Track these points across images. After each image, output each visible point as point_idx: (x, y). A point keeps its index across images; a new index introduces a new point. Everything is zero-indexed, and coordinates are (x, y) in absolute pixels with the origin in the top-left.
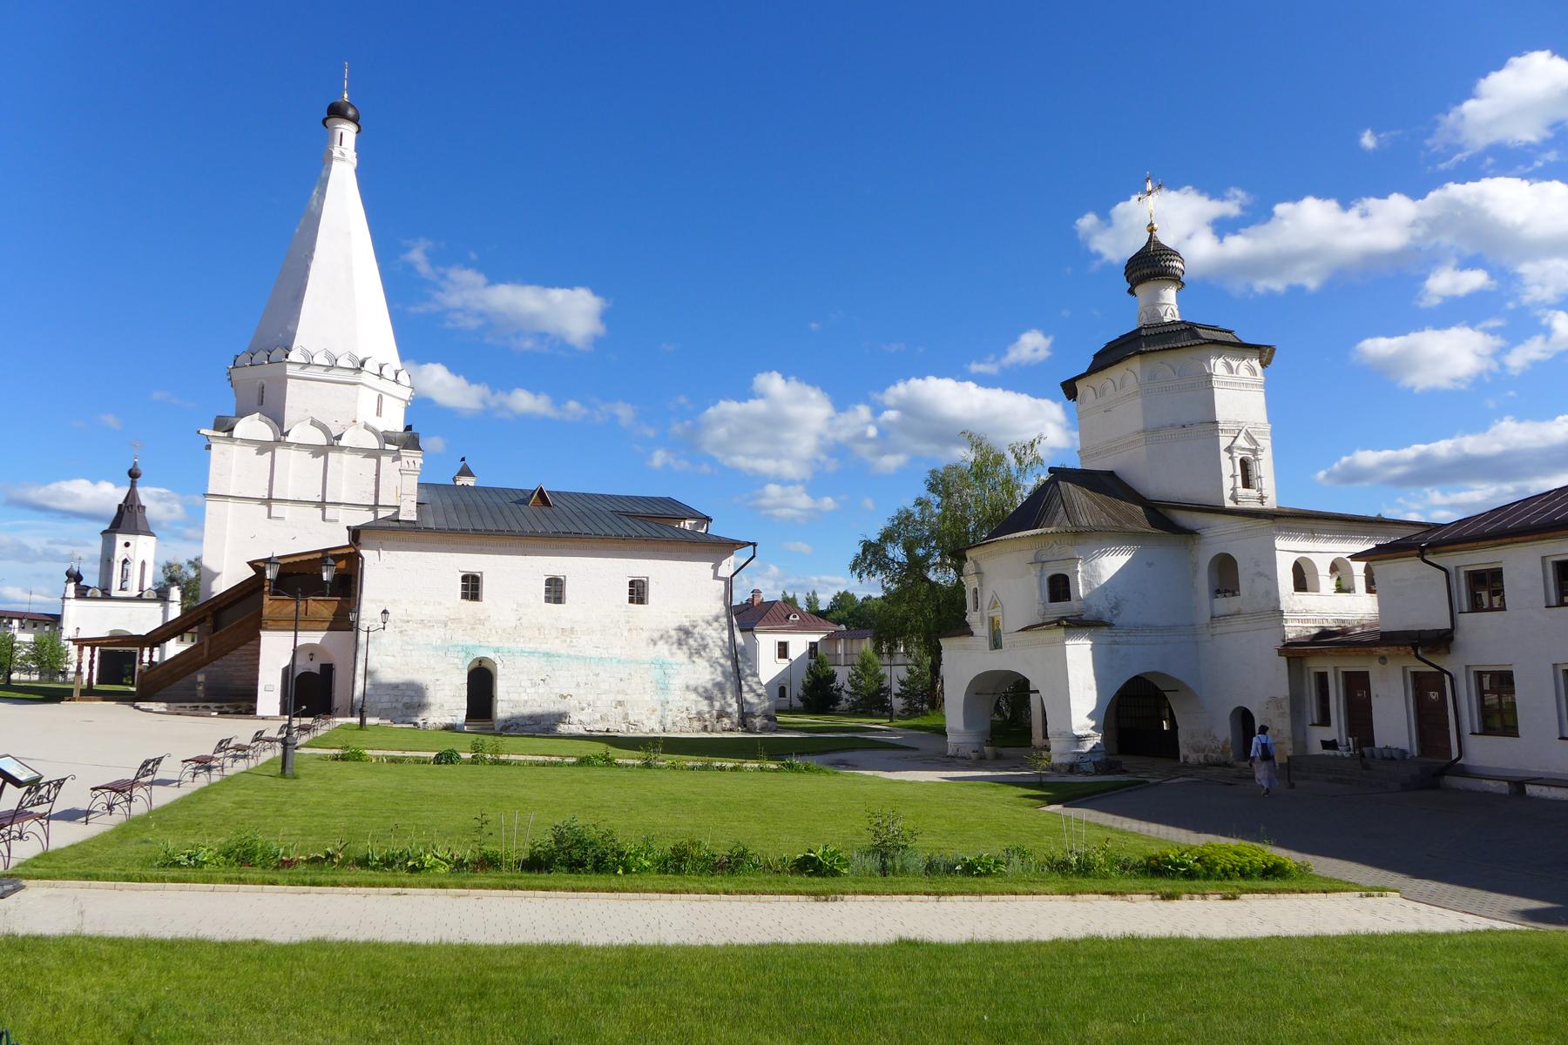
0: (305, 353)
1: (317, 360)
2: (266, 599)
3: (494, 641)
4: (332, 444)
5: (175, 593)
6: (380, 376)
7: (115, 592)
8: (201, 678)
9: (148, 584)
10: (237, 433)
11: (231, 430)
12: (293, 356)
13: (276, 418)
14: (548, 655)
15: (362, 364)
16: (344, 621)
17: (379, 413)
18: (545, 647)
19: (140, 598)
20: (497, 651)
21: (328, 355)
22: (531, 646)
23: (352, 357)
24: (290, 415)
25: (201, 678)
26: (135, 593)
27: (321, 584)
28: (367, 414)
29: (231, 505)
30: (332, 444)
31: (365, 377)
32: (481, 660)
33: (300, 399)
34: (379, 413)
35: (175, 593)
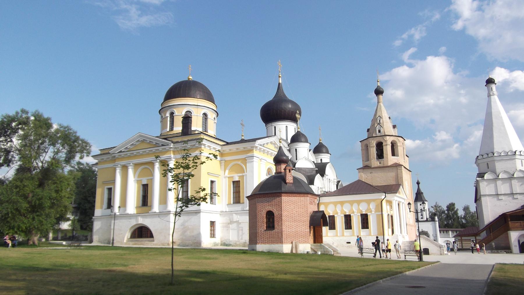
0: (498, 153)
1: (502, 154)
2: (510, 222)
4: (511, 177)
5: (436, 218)
6: (521, 155)
7: (420, 219)
8: (493, 244)
10: (485, 178)
11: (483, 177)
12: (495, 155)
13: (494, 172)
15: (515, 152)
17: (522, 166)
19: (427, 221)
21: (505, 152)
24: (498, 171)
25: (493, 244)
26: (425, 219)
30: (511, 177)
31: (517, 157)
33: (500, 166)
34: (522, 166)
35: (436, 218)
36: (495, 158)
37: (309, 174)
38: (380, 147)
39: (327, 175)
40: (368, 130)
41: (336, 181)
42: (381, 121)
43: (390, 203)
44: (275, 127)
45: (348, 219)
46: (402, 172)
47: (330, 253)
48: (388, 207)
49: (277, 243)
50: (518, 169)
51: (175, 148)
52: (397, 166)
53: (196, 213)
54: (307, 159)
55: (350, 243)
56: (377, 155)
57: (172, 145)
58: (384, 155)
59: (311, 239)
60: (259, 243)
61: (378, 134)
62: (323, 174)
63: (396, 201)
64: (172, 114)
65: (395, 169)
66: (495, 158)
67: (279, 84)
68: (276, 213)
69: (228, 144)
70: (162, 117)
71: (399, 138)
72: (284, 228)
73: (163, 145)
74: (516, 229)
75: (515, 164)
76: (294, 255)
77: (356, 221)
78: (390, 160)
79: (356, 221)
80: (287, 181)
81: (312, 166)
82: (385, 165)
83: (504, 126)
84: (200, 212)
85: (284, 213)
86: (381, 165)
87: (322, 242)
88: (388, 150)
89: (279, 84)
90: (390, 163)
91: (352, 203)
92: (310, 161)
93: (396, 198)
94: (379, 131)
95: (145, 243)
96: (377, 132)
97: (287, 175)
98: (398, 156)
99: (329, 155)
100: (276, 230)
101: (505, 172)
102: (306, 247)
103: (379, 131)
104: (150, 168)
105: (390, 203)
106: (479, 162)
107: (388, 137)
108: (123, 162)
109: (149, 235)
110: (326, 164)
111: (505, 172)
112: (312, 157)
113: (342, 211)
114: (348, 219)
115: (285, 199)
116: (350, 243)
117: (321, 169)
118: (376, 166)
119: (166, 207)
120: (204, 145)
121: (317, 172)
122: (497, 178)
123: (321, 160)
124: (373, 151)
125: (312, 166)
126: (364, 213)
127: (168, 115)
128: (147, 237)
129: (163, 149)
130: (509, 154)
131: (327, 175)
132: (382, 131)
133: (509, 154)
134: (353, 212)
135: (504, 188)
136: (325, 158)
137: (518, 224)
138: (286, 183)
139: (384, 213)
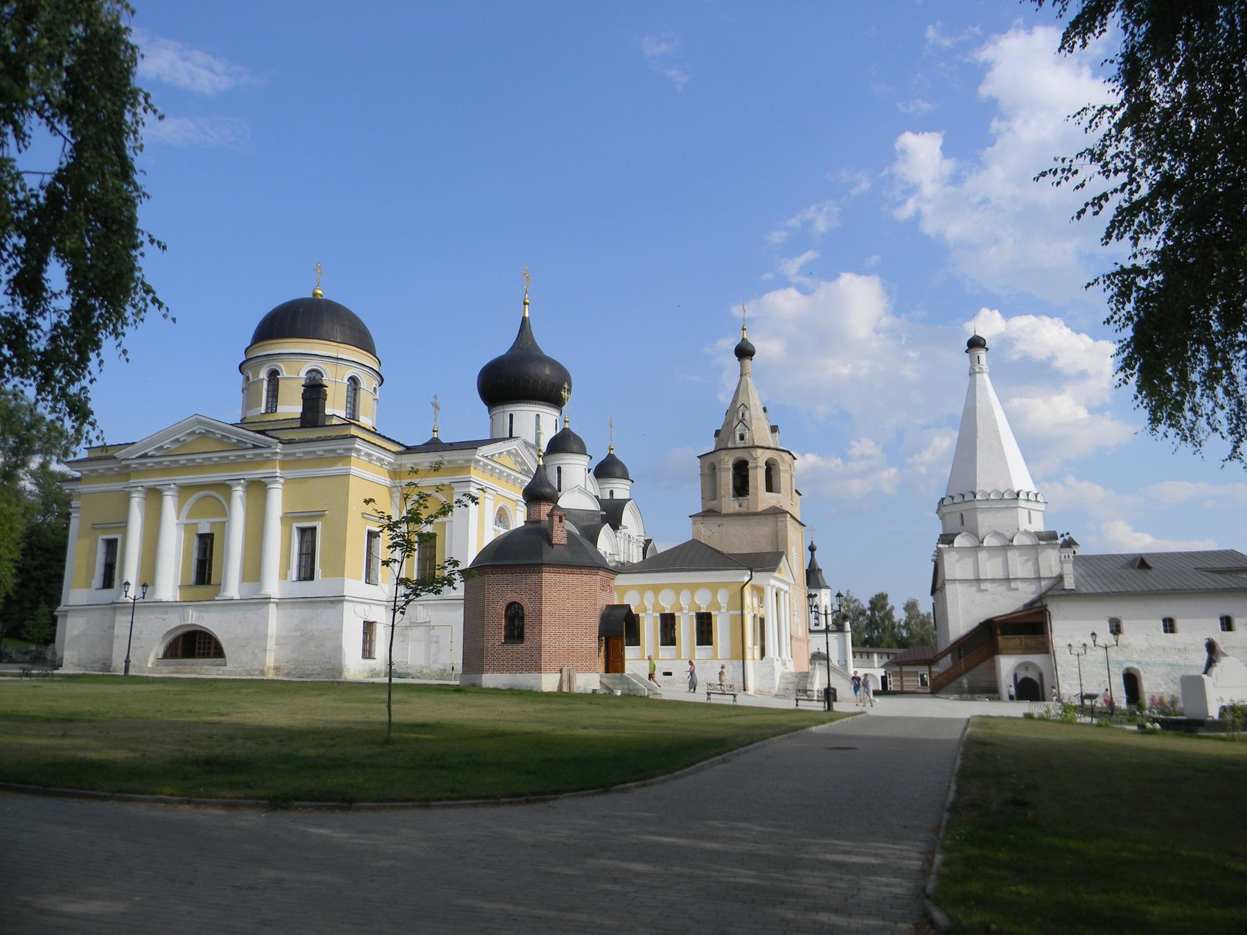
0: (984, 493)
1: (992, 497)
2: (1000, 638)
3: (1136, 657)
6: (1028, 500)
8: (965, 681)
9: (830, 622)
10: (956, 544)
12: (978, 497)
13: (974, 533)
14: (1171, 665)
16: (1044, 648)
18: (1169, 660)
20: (1139, 663)
21: (997, 492)
22: (1160, 660)
23: (1011, 492)
24: (982, 531)
25: (965, 681)
27: (1029, 627)
28: (1024, 525)
29: (958, 586)
30: (1008, 546)
31: (1022, 503)
32: (1128, 669)
33: (986, 522)
36: (978, 505)
37: (586, 523)
38: (741, 470)
39: (626, 528)
40: (717, 433)
41: (642, 539)
42: (747, 416)
43: (759, 591)
44: (511, 416)
45: (668, 623)
46: (786, 527)
47: (641, 693)
48: (755, 601)
49: (529, 671)
50: (1022, 529)
51: (285, 455)
52: (776, 513)
53: (332, 602)
54: (583, 491)
55: (670, 674)
56: (735, 488)
57: (279, 448)
58: (750, 489)
59: (600, 663)
60: (487, 672)
61: (739, 443)
62: (616, 524)
63: (773, 586)
64: (274, 374)
65: (770, 521)
66: (978, 505)
67: (524, 319)
68: (528, 607)
69: (409, 450)
70: (248, 378)
71: (783, 454)
72: (545, 640)
73: (255, 447)
74: (1011, 651)
75: (1017, 518)
76: (563, 697)
77: (686, 629)
78: (762, 499)
79: (686, 629)
80: (555, 541)
81: (593, 506)
82: (752, 510)
83: (999, 438)
84: (342, 601)
85: (546, 609)
86: (743, 510)
87: (622, 671)
88: (758, 477)
89: (524, 319)
90: (762, 507)
91: (677, 589)
92: (588, 494)
93: (773, 582)
94: (742, 438)
95: (203, 669)
96: (738, 437)
97: (555, 528)
98: (779, 492)
99: (629, 483)
100: (527, 643)
101: (996, 534)
102: (589, 680)
103: (742, 438)
104: (221, 498)
105: (759, 591)
106: (944, 510)
107: (760, 451)
108: (151, 481)
109: (212, 651)
110: (623, 502)
111: (996, 534)
112: (592, 486)
113: (656, 605)
114: (668, 623)
115: (549, 578)
116: (670, 674)
117: (612, 513)
118: (731, 511)
119: (260, 588)
120: (358, 451)
121: (605, 520)
122: (979, 546)
123: (612, 493)
124: (727, 479)
125: (593, 506)
126: (703, 611)
127: (263, 375)
128: (208, 656)
129: (255, 455)
130: (1006, 496)
131: (626, 528)
132: (747, 437)
133: (1006, 496)
134: (681, 609)
135: (991, 567)
136: (621, 489)
137: (1015, 641)
138: (552, 545)
139: (746, 612)
